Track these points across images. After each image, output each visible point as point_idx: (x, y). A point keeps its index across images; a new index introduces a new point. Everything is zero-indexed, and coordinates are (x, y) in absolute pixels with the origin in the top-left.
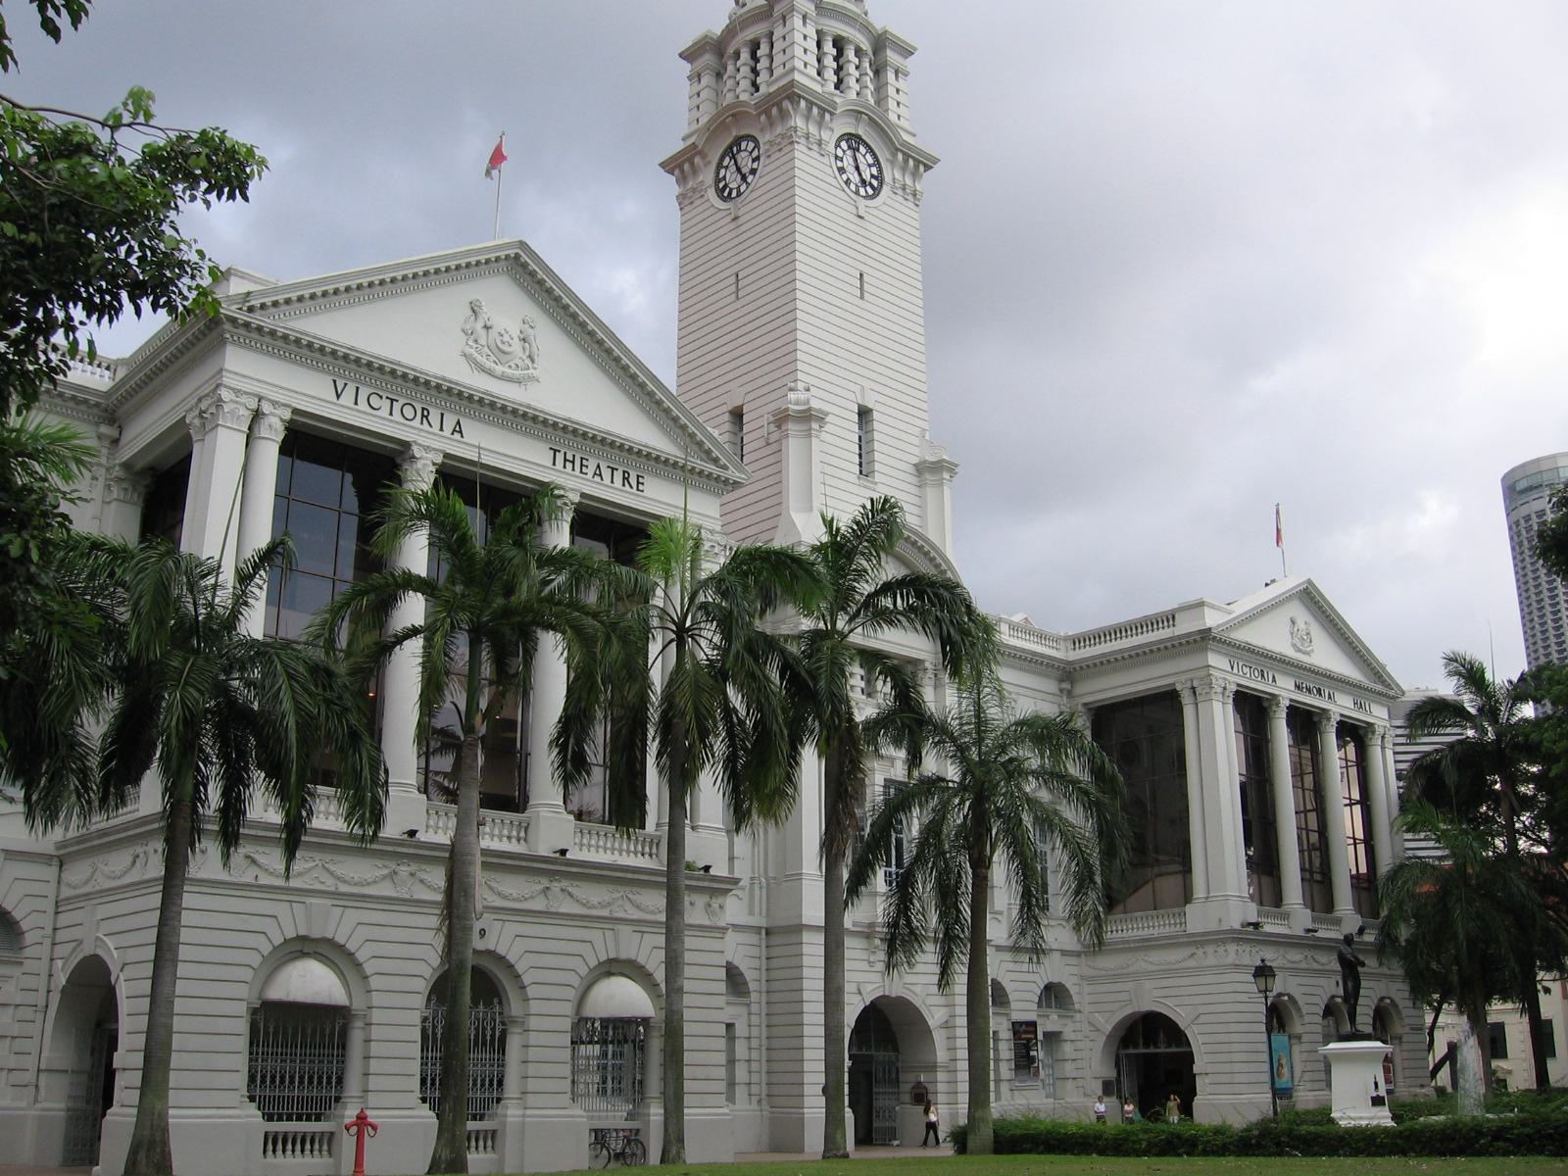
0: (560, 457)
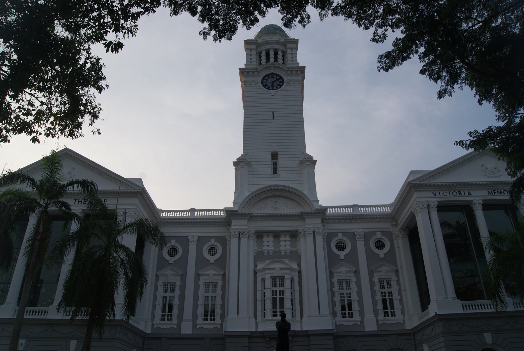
0: (77, 201)
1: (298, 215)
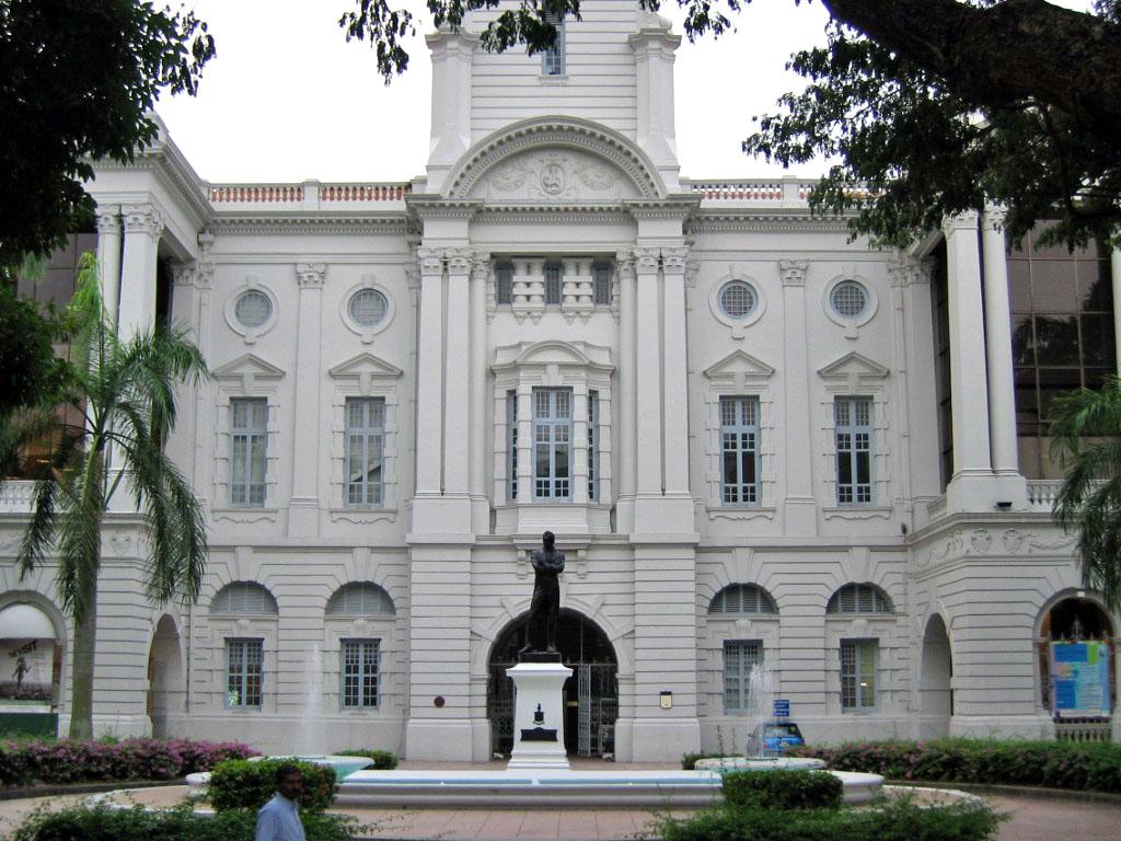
1: (617, 209)
